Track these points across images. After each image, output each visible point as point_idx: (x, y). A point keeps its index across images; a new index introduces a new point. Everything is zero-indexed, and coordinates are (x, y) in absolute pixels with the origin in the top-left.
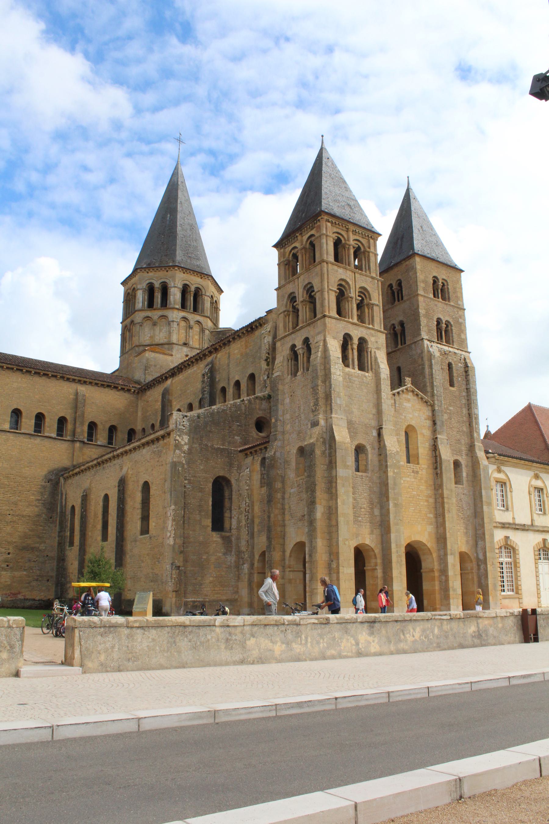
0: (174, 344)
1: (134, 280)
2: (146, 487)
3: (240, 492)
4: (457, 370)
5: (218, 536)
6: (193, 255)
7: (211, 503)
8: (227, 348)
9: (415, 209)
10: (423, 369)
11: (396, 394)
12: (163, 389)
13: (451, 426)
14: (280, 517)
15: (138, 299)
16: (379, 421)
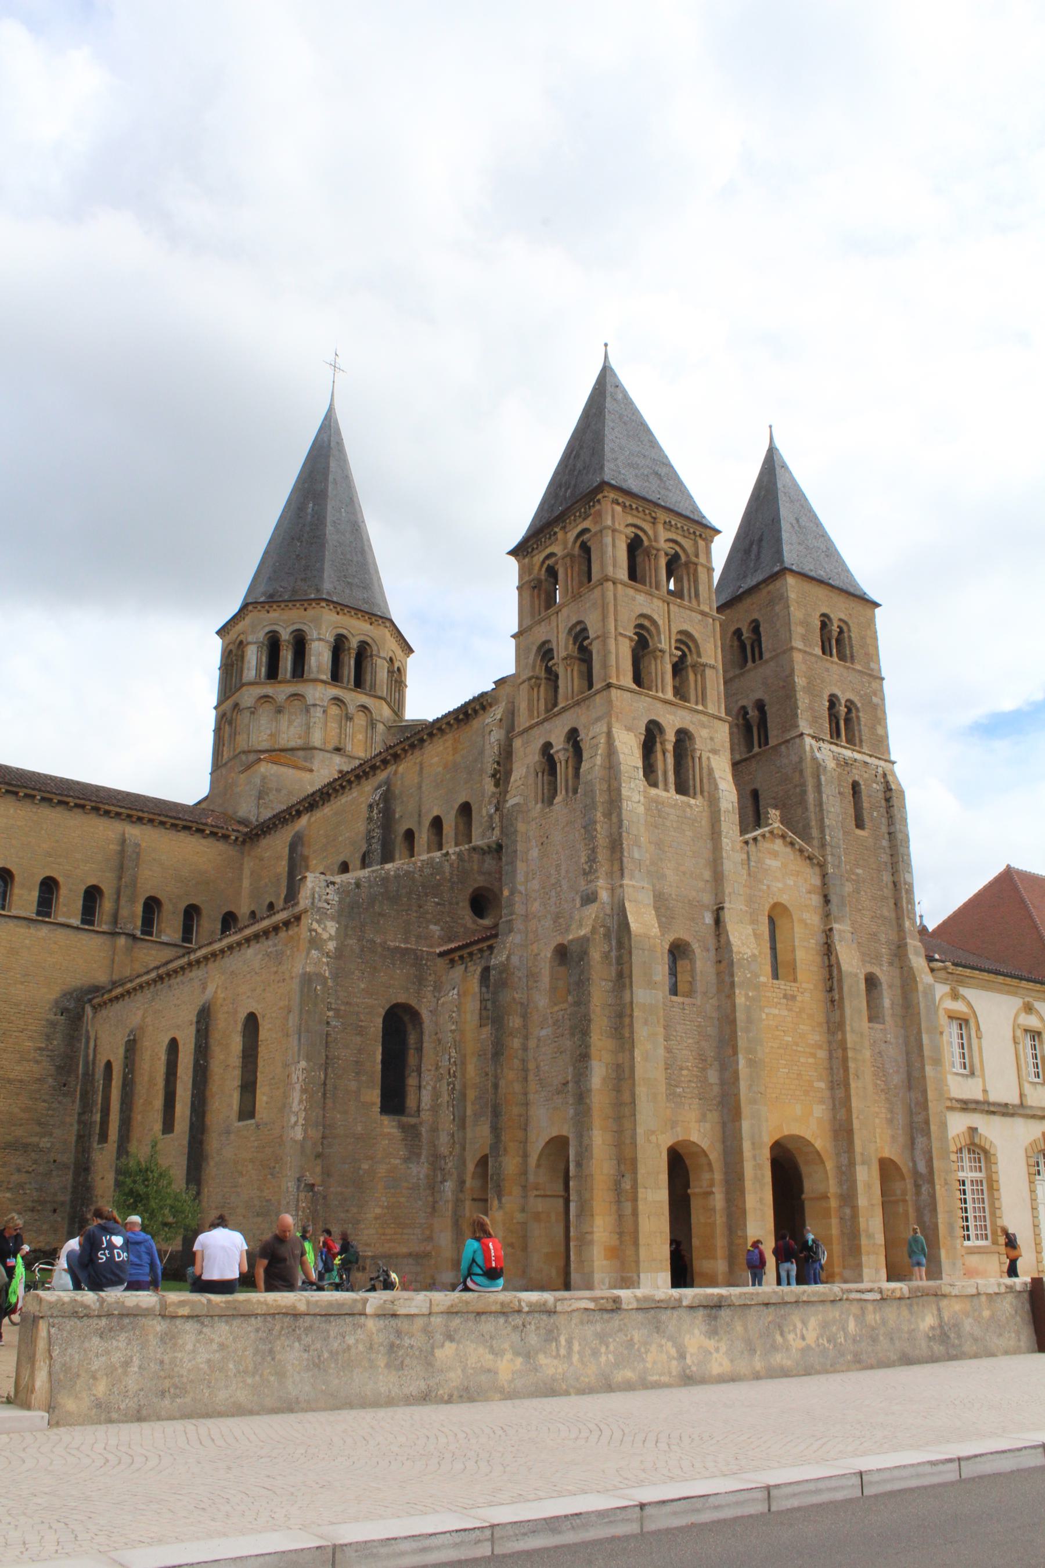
0: (315, 748)
1: (240, 626)
2: (252, 1023)
3: (440, 1036)
4: (870, 796)
5: (394, 1123)
6: (356, 580)
7: (379, 1057)
8: (417, 753)
9: (784, 487)
10: (804, 792)
11: (751, 841)
12: (292, 833)
13: (860, 907)
14: (517, 1087)
15: (249, 662)
16: (716, 895)
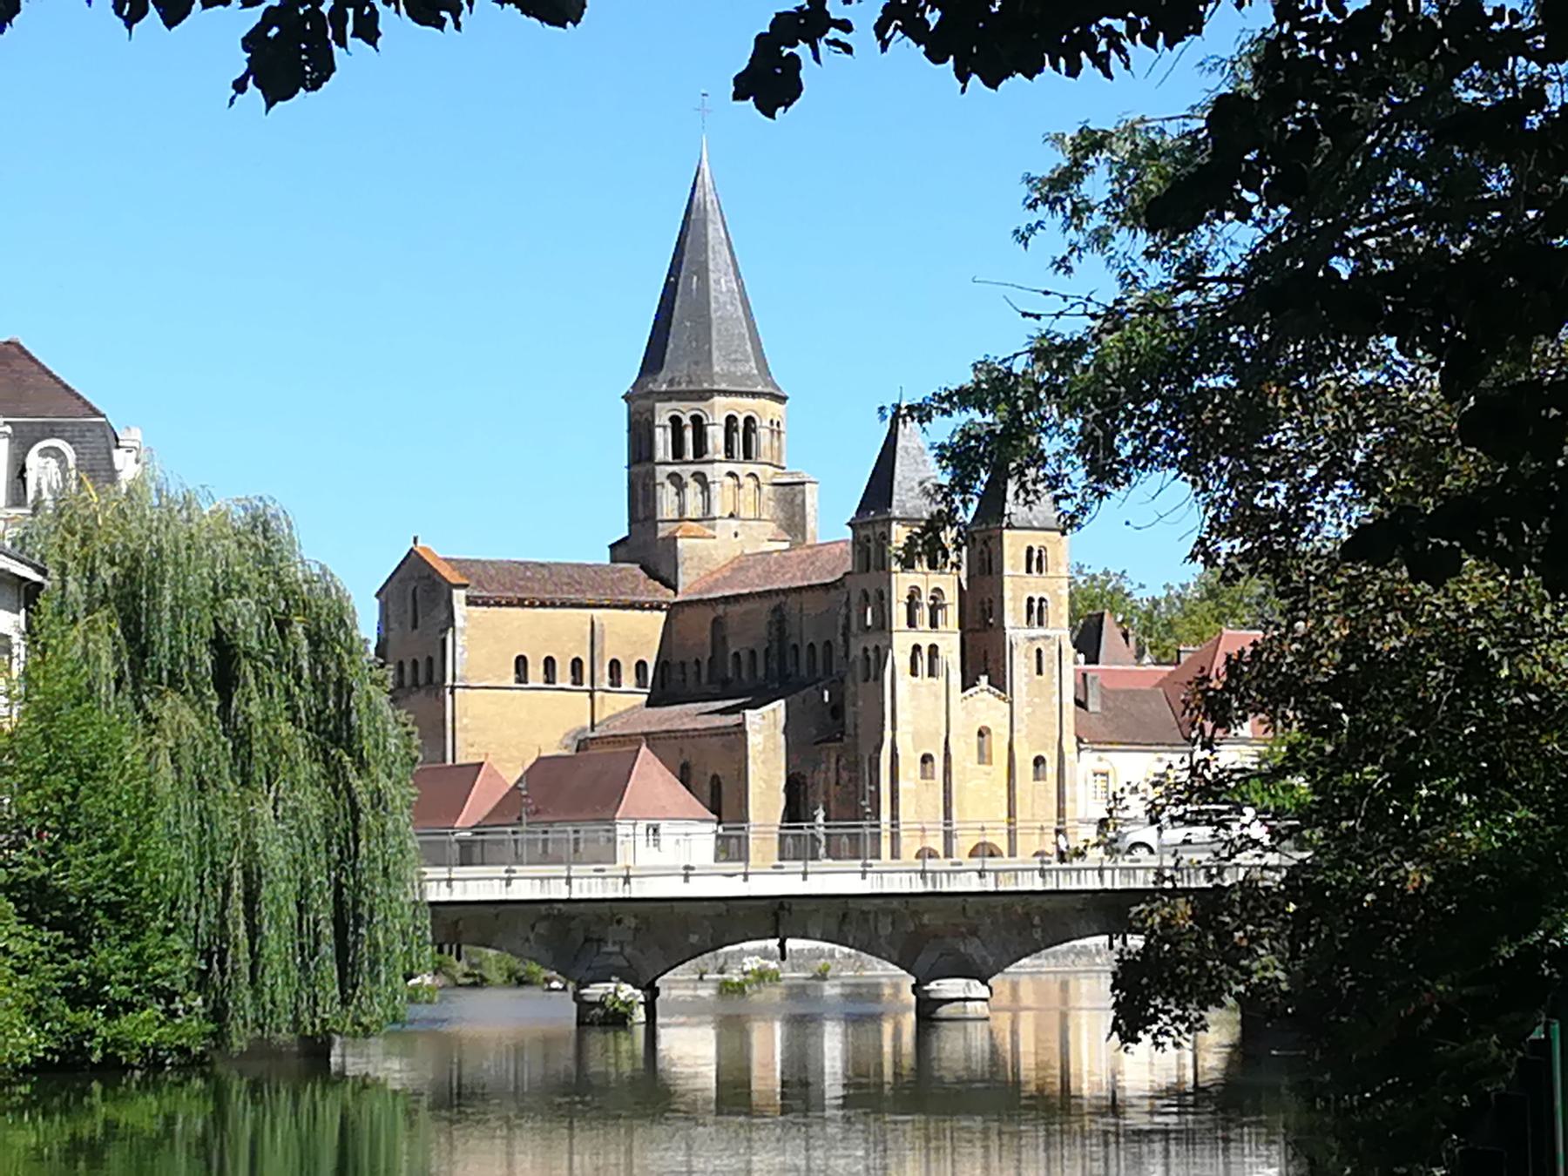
12: (712, 616)
